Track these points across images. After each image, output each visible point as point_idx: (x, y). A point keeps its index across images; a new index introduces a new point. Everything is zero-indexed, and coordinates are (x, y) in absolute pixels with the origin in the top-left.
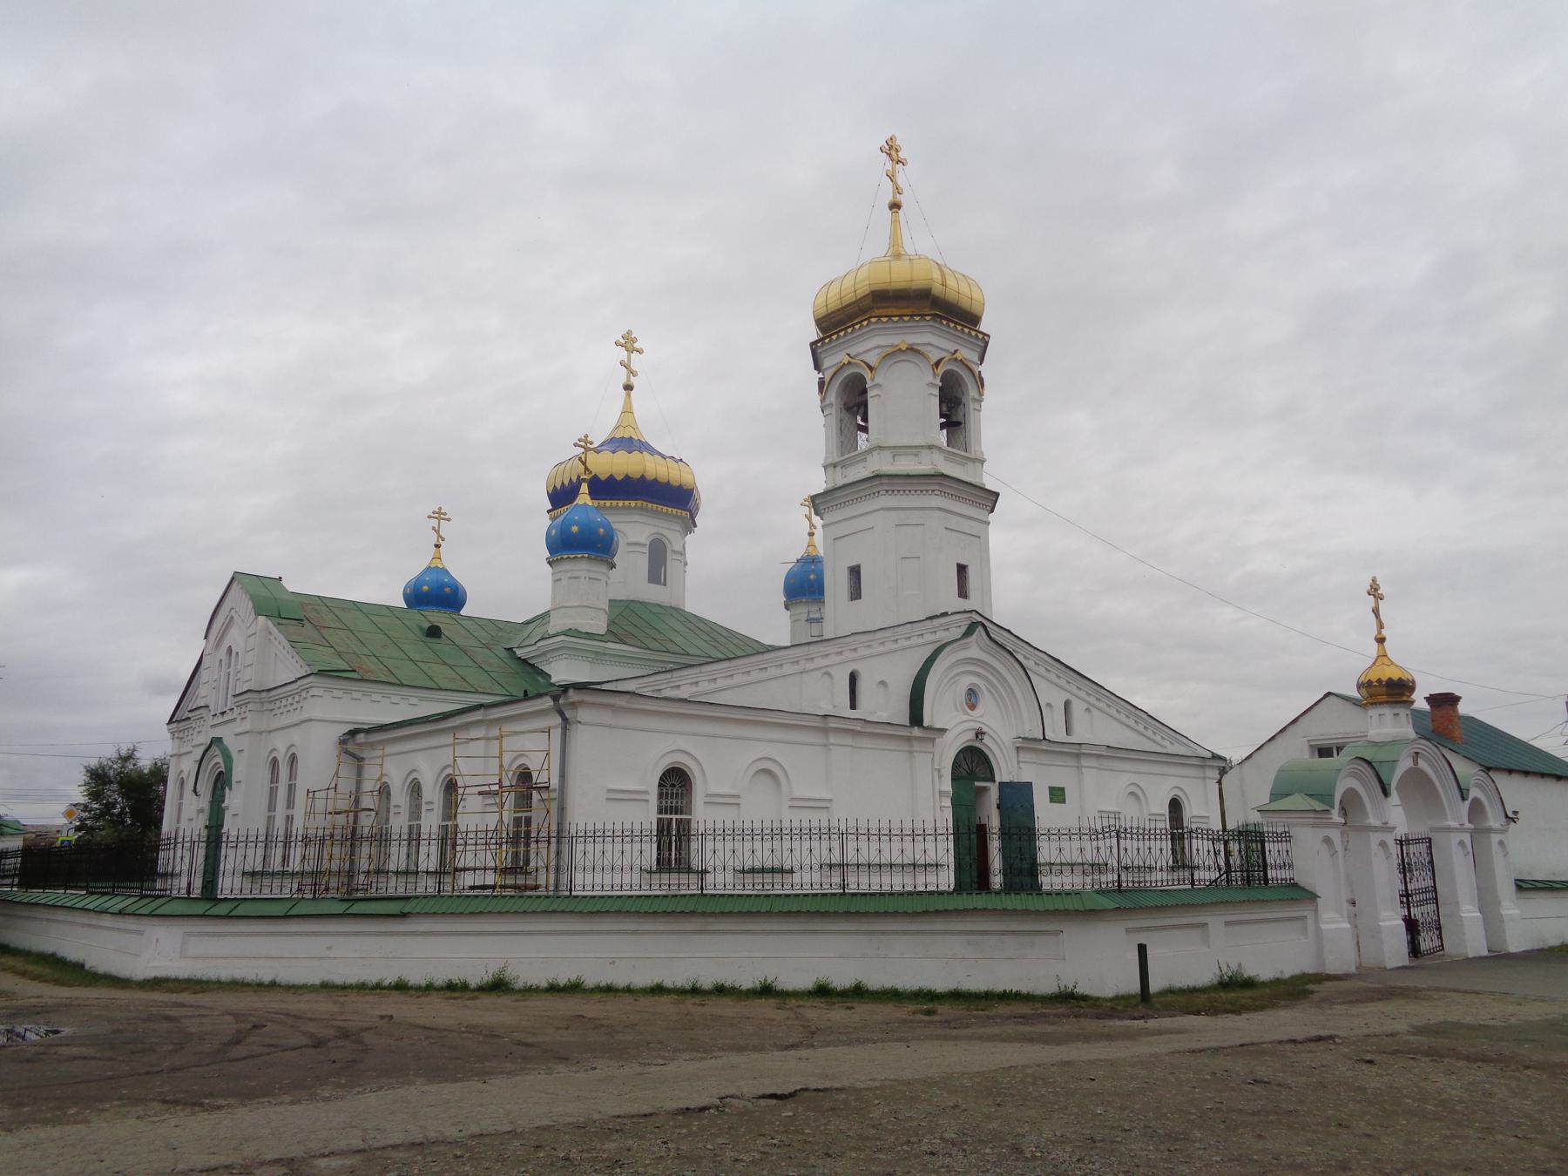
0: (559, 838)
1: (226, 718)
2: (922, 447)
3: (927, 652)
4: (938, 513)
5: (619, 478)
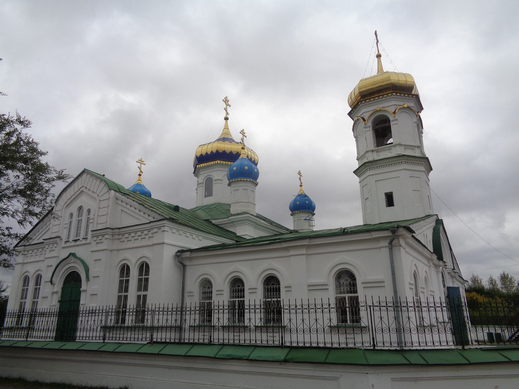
1: (78, 243)
2: (415, 146)
5: (234, 153)
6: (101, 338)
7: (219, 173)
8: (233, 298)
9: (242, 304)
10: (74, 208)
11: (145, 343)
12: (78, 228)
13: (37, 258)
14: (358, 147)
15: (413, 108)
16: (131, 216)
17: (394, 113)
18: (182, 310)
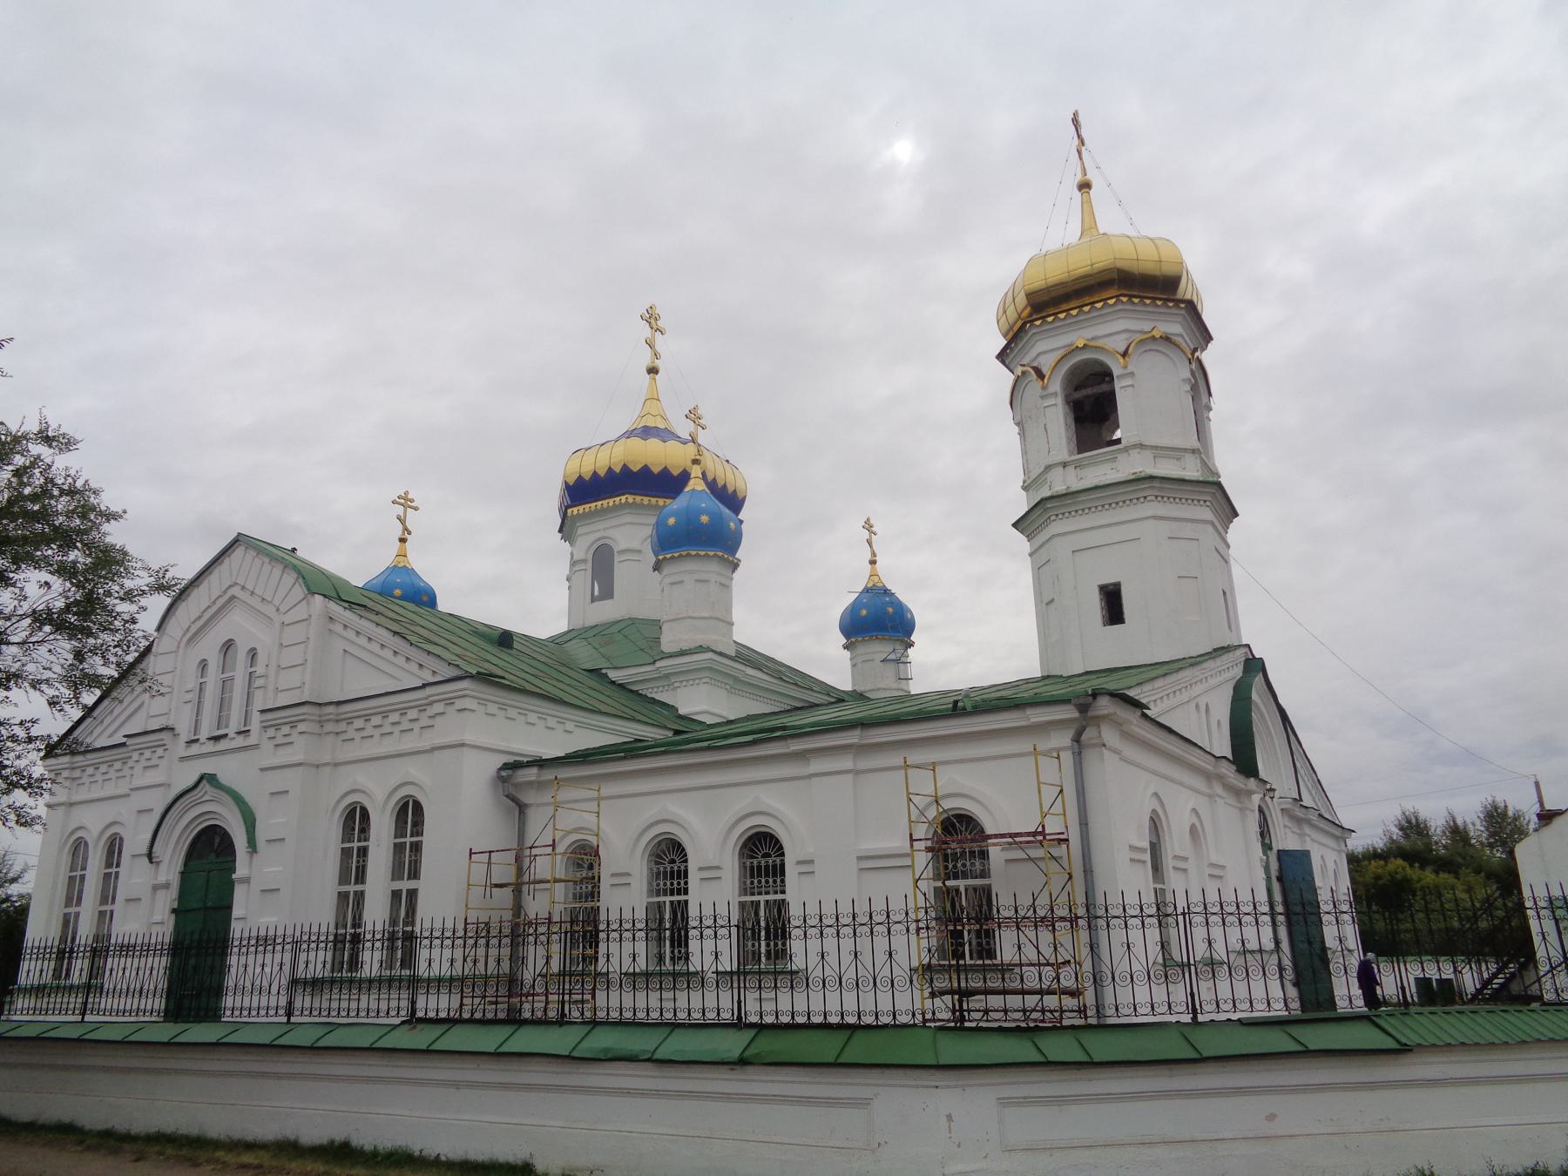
0: (1091, 918)
2: (1185, 450)
3: (1227, 693)
4: (1210, 528)
5: (675, 473)
6: (281, 1012)
7: (630, 529)
8: (658, 895)
9: (680, 910)
10: (209, 647)
11: (397, 1021)
12: (223, 704)
13: (110, 790)
14: (1024, 452)
15: (1179, 340)
16: (371, 665)
17: (1125, 354)
18: (518, 932)
